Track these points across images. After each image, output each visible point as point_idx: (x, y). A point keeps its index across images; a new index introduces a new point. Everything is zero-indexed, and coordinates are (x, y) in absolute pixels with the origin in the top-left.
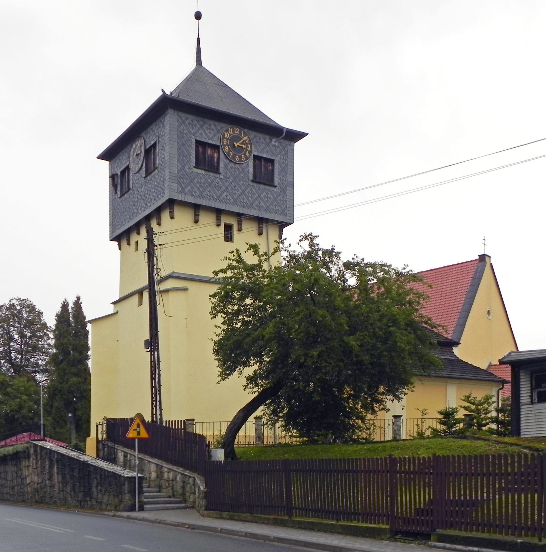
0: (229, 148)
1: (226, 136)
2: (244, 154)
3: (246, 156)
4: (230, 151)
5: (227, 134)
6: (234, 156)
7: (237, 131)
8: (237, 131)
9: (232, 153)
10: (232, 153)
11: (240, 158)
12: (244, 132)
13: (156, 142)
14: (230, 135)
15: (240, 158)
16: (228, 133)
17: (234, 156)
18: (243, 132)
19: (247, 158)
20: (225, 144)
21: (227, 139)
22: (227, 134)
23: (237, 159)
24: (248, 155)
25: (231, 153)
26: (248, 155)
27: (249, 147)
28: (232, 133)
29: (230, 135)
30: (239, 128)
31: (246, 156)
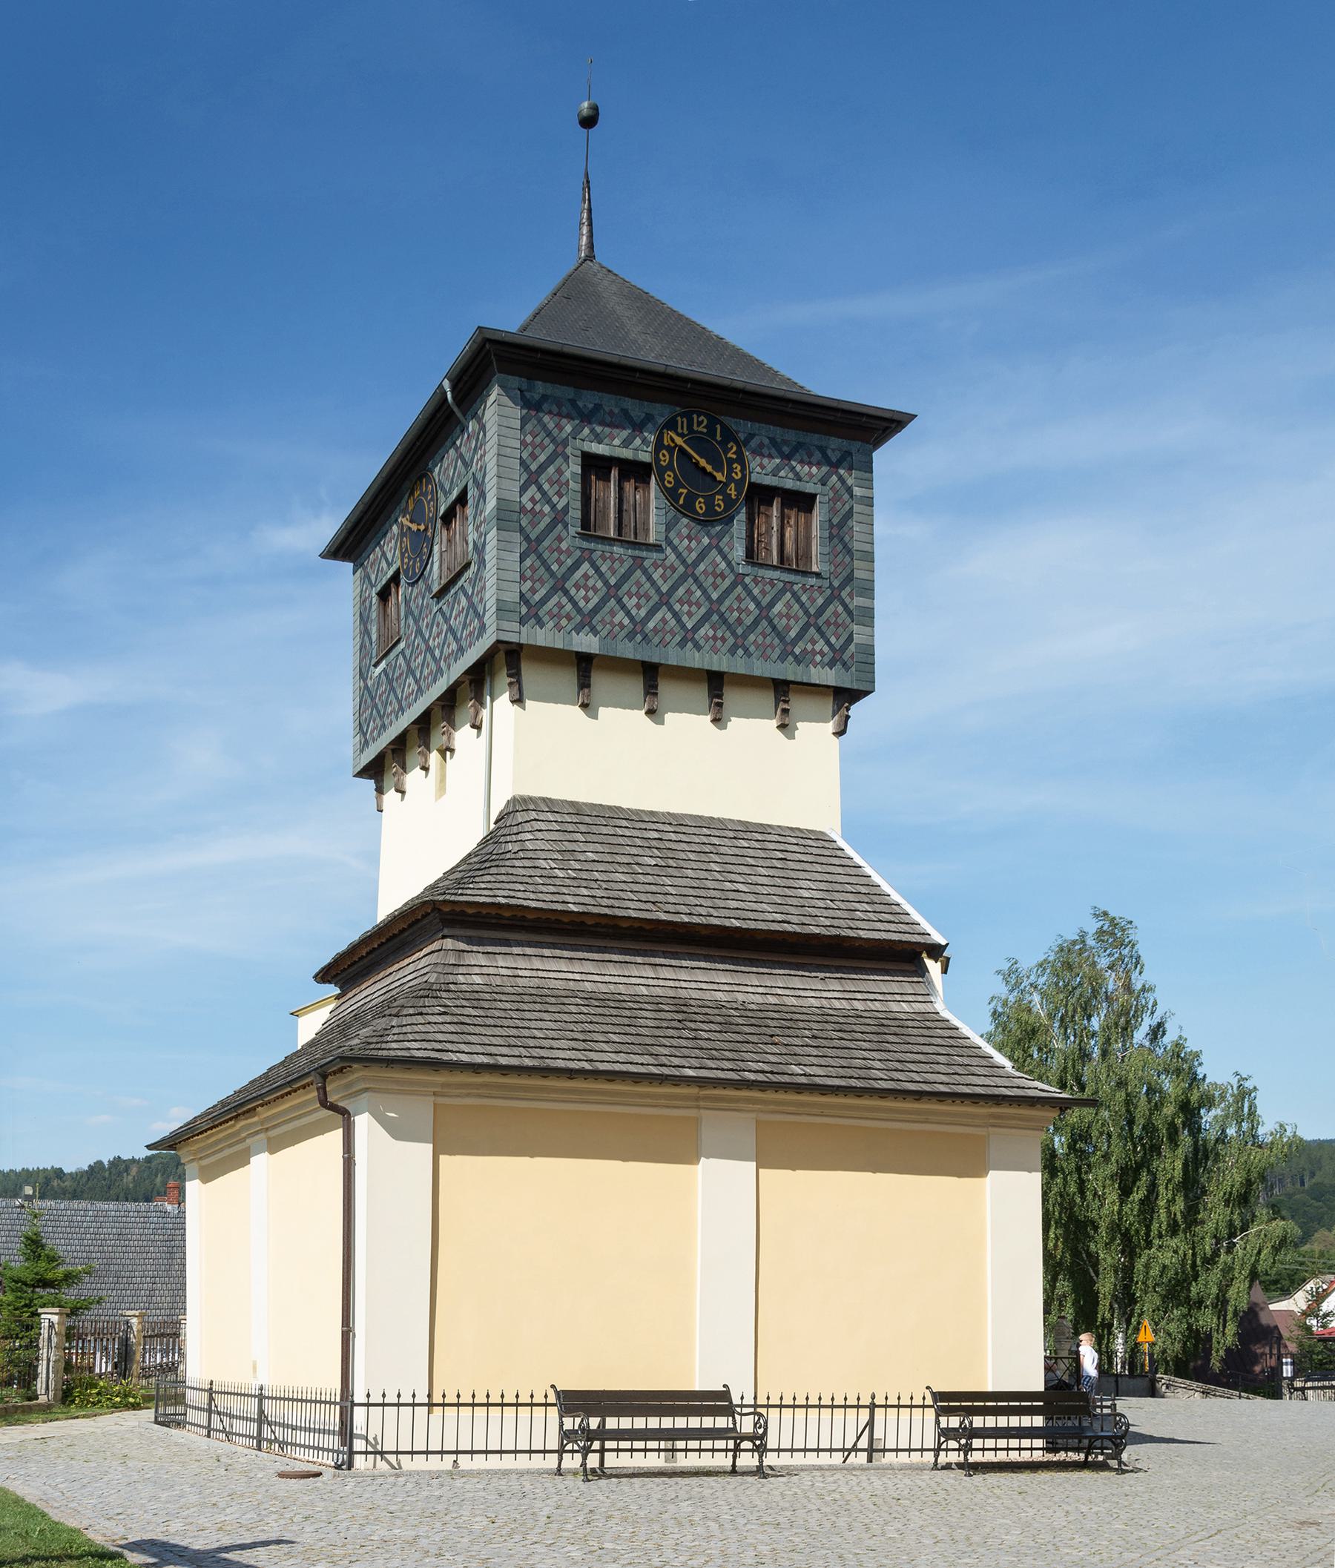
0: (675, 477)
2: (722, 492)
3: (727, 499)
4: (678, 484)
6: (691, 499)
7: (700, 423)
8: (700, 423)
9: (685, 491)
10: (685, 491)
11: (710, 502)
12: (724, 427)
15: (710, 502)
17: (691, 499)
18: (718, 426)
19: (729, 503)
20: (664, 464)
23: (700, 506)
24: (733, 493)
25: (681, 490)
26: (733, 493)
27: (738, 470)
30: (706, 415)
31: (727, 499)
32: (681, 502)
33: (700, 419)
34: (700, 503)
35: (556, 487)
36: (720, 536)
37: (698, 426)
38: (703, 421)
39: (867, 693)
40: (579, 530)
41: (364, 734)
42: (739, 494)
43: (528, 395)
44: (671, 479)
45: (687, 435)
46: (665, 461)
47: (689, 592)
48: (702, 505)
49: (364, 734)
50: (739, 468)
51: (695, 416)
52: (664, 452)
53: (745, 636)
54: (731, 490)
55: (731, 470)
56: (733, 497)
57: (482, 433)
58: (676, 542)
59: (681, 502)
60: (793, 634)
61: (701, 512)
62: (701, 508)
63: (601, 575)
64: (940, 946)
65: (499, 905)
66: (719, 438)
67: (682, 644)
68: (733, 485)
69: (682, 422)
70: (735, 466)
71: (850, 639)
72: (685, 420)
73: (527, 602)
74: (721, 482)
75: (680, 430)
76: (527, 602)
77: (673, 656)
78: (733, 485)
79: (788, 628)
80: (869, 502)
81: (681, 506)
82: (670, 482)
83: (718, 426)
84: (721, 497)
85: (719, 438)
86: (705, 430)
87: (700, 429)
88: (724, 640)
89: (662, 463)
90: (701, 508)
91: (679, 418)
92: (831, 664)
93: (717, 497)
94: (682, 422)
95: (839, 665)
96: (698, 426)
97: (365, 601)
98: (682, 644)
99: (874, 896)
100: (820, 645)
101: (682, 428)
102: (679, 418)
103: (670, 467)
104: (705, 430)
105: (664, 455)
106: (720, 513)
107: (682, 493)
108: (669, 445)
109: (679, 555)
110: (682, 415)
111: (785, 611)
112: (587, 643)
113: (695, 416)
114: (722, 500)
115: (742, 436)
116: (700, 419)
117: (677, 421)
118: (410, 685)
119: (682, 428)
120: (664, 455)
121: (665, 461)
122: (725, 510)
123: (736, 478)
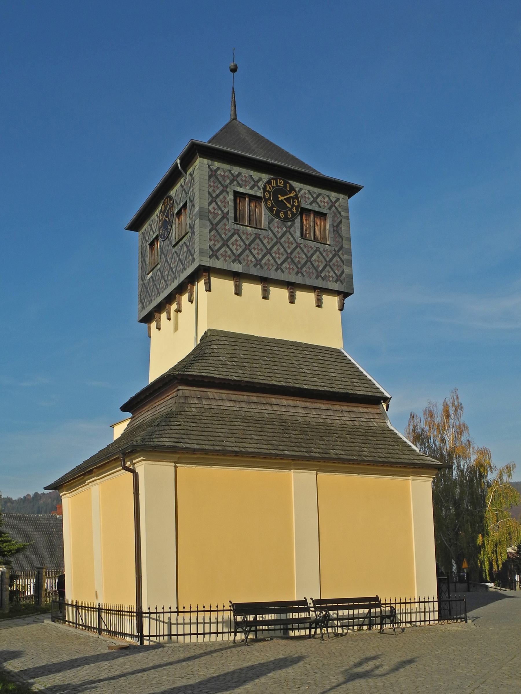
0: (272, 203)
1: (268, 189)
3: (292, 213)
4: (273, 206)
5: (270, 187)
7: (280, 183)
8: (280, 183)
10: (276, 209)
11: (286, 214)
13: (186, 202)
14: (273, 187)
15: (286, 214)
16: (270, 186)
18: (288, 185)
21: (269, 192)
22: (270, 187)
23: (282, 215)
24: (295, 211)
25: (274, 208)
26: (295, 211)
27: (296, 202)
28: (275, 186)
29: (273, 187)
30: (283, 180)
31: (292, 213)
32: (274, 213)
33: (281, 181)
34: (282, 214)
35: (223, 204)
36: (290, 227)
37: (280, 184)
38: (282, 182)
39: (352, 294)
40: (233, 221)
41: (143, 304)
42: (297, 211)
43: (211, 167)
44: (270, 204)
45: (276, 187)
46: (267, 196)
47: (279, 249)
48: (283, 215)
49: (143, 304)
50: (297, 201)
51: (279, 180)
52: (267, 193)
53: (301, 268)
54: (294, 209)
55: (293, 202)
56: (295, 212)
57: (193, 181)
58: (272, 228)
59: (274, 213)
60: (320, 268)
61: (282, 217)
62: (282, 216)
63: (242, 240)
64: (388, 398)
65: (203, 376)
66: (288, 189)
67: (276, 270)
68: (294, 208)
69: (274, 182)
70: (295, 200)
71: (343, 272)
72: (275, 181)
73: (212, 250)
74: (289, 207)
75: (273, 185)
76: (212, 250)
77: (273, 275)
78: (294, 208)
79: (318, 266)
80: (348, 218)
81: (274, 214)
82: (269, 205)
83: (288, 185)
84: (290, 212)
85: (288, 189)
86: (283, 186)
87: (281, 185)
88: (293, 269)
89: (266, 197)
90: (282, 216)
91: (272, 180)
92: (336, 281)
93: (289, 212)
94: (274, 182)
95: (339, 282)
96: (280, 184)
97: (143, 248)
98: (276, 270)
99: (361, 376)
100: (332, 274)
101: (274, 184)
102: (272, 180)
103: (269, 199)
104: (283, 186)
105: (267, 194)
106: (290, 218)
107: (275, 209)
108: (269, 190)
109: (274, 234)
110: (273, 179)
111: (317, 259)
112: (237, 267)
113: (279, 180)
114: (290, 213)
115: (297, 189)
116: (281, 181)
117: (272, 182)
118: (162, 283)
119: (274, 184)
120: (267, 194)
121: (267, 196)
122: (292, 217)
123: (296, 205)
